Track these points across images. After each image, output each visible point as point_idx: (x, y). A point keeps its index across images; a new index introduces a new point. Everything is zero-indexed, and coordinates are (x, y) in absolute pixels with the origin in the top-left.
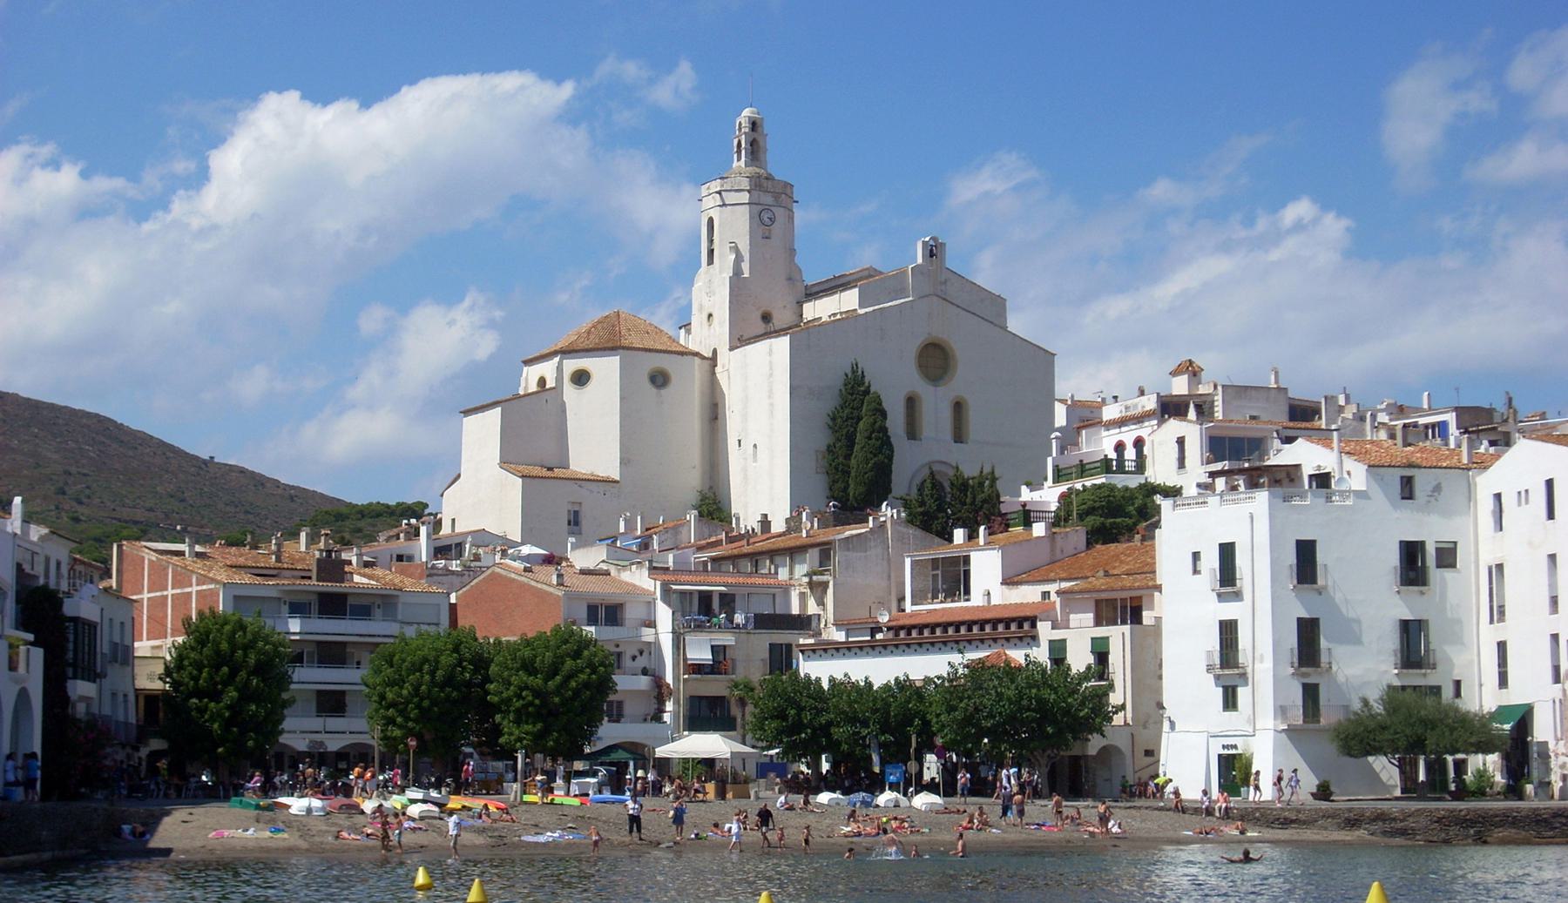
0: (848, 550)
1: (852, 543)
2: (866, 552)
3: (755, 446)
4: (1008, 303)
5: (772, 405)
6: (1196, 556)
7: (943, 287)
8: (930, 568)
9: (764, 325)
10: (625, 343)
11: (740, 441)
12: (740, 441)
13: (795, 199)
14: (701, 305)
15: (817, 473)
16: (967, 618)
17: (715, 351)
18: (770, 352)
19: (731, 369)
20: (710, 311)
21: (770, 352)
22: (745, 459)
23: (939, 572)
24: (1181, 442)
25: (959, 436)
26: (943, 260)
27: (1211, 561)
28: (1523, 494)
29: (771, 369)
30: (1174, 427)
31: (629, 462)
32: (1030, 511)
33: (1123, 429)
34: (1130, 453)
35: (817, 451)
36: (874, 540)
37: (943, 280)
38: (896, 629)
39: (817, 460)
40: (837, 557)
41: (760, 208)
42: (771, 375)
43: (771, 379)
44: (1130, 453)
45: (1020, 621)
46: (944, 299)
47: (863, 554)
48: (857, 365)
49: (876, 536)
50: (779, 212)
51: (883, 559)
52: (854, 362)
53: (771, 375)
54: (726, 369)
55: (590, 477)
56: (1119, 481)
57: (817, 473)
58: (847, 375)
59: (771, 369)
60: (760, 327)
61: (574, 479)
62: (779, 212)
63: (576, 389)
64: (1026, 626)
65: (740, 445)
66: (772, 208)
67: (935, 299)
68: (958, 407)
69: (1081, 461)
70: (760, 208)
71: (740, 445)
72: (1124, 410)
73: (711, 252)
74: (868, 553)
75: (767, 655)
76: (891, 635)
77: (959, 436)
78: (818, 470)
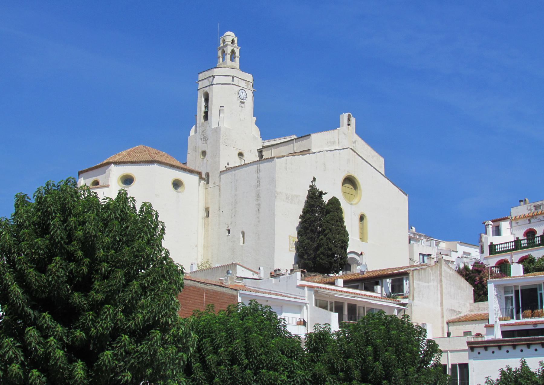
0: (420, 280)
3: (243, 233)
5: (259, 205)
7: (354, 145)
11: (229, 231)
12: (229, 231)
14: (196, 147)
15: (290, 251)
17: (208, 175)
18: (258, 171)
19: (221, 185)
20: (204, 149)
21: (258, 171)
29: (259, 181)
33: (532, 220)
35: (290, 236)
37: (354, 141)
39: (290, 242)
42: (259, 186)
43: (258, 188)
47: (427, 284)
49: (433, 272)
51: (437, 290)
59: (259, 181)
65: (229, 233)
68: (362, 218)
71: (229, 233)
72: (533, 209)
73: (206, 113)
74: (430, 284)
77: (363, 237)
78: (291, 250)
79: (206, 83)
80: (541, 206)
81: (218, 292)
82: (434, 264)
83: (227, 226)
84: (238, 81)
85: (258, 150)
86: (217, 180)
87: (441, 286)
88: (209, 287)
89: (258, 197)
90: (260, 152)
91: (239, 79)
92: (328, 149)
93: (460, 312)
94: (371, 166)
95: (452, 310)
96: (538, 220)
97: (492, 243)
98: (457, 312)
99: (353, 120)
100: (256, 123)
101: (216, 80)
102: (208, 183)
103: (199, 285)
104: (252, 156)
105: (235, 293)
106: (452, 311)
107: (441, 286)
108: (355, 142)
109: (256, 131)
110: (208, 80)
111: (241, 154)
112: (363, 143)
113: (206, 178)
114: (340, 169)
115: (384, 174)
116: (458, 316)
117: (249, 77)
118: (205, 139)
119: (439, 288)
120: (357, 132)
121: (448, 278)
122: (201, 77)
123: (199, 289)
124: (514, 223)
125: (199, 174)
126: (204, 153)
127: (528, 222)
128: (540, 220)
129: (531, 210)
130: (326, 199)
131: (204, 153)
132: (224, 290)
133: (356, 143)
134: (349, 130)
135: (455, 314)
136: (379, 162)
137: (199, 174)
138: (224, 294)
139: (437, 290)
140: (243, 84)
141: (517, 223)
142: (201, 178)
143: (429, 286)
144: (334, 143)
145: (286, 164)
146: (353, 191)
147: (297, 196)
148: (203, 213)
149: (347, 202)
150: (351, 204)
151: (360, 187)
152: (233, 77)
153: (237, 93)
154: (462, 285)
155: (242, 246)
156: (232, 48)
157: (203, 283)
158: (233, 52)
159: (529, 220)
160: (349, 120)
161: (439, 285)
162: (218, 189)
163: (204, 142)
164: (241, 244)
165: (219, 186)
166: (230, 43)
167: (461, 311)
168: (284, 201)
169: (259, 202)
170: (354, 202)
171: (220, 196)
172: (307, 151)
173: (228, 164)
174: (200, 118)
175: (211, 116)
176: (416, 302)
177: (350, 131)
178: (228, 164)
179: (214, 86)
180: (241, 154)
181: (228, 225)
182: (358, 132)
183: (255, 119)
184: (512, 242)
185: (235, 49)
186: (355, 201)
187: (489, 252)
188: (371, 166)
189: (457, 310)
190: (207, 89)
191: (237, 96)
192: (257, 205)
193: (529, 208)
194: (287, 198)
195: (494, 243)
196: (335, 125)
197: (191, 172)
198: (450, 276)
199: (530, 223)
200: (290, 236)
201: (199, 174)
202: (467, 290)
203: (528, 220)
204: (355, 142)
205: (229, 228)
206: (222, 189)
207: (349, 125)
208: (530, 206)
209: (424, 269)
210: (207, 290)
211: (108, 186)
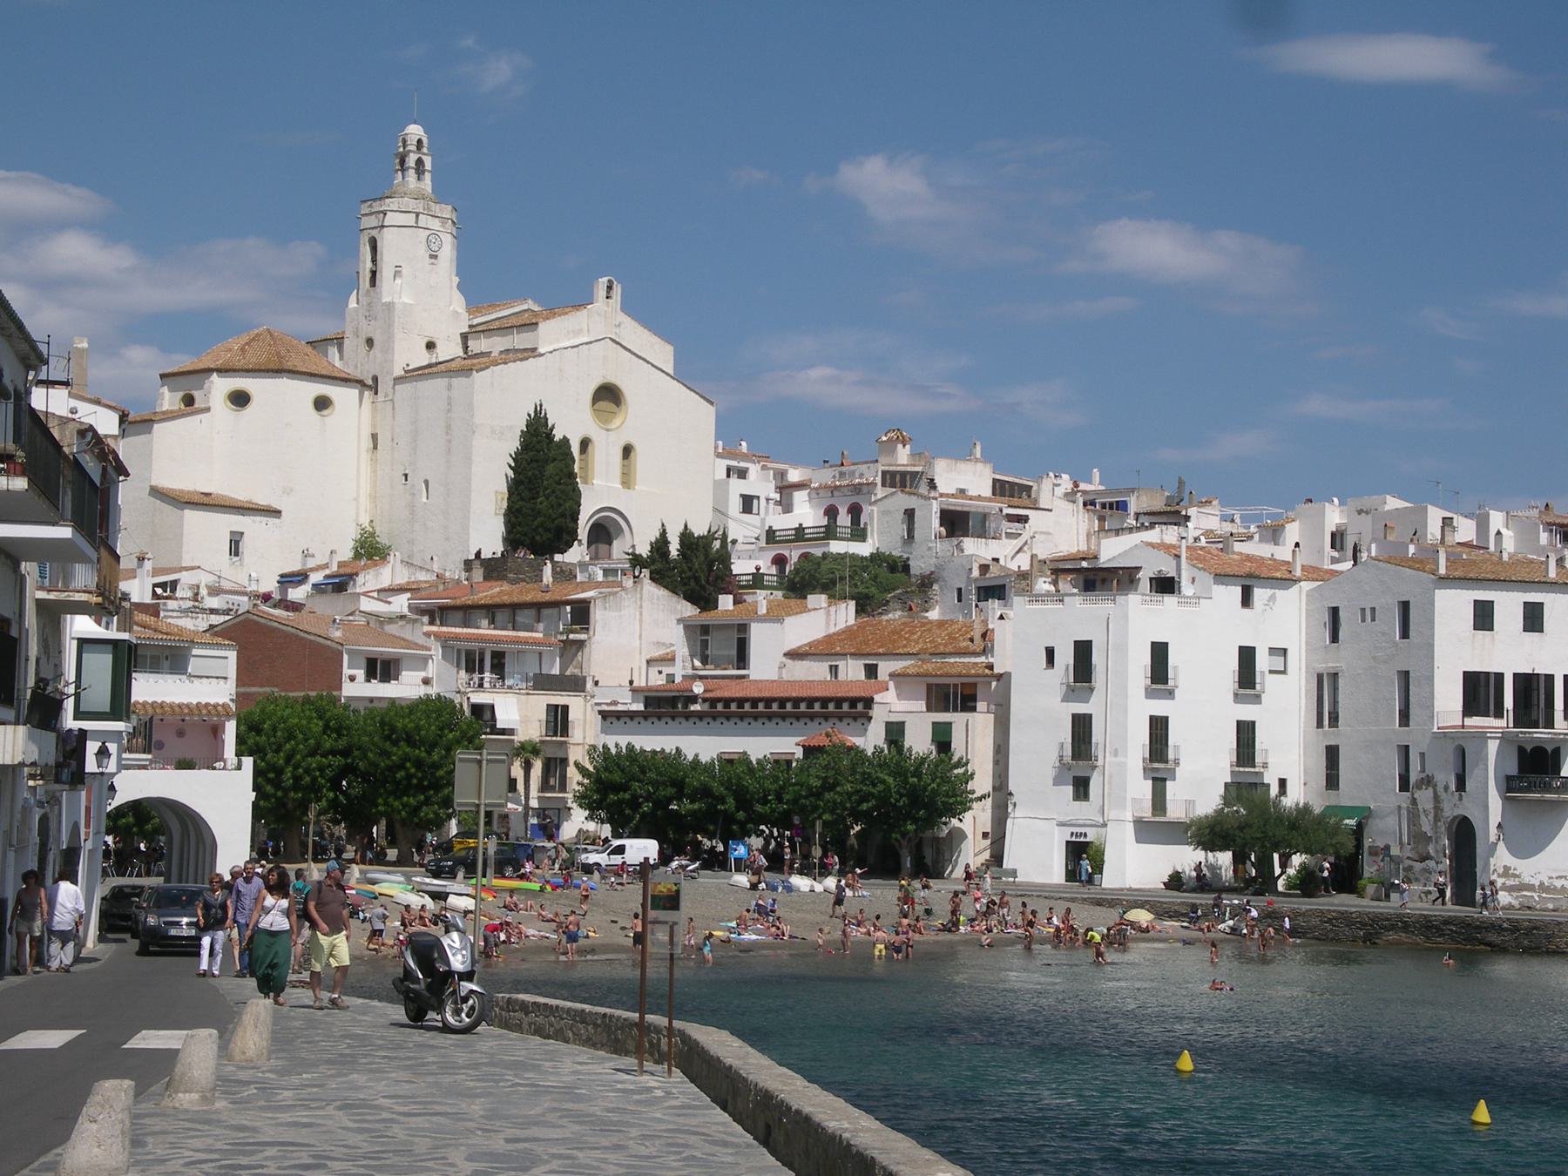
0: (605, 609)
3: (426, 482)
6: (1050, 653)
8: (699, 633)
9: (428, 356)
10: (289, 365)
11: (406, 475)
12: (406, 475)
15: (496, 514)
16: (766, 694)
17: (375, 379)
18: (449, 388)
19: (395, 400)
21: (449, 388)
24: (910, 514)
25: (627, 480)
27: (1065, 657)
28: (1368, 613)
29: (449, 404)
30: (902, 501)
31: (291, 490)
32: (763, 574)
33: (836, 493)
34: (844, 519)
35: (496, 492)
38: (713, 702)
40: (598, 614)
42: (449, 411)
44: (844, 519)
45: (853, 702)
46: (618, 343)
47: (617, 614)
48: (541, 406)
52: (538, 404)
53: (449, 411)
54: (390, 398)
55: (248, 505)
56: (836, 547)
57: (496, 514)
58: (529, 415)
59: (449, 404)
61: (238, 508)
63: (233, 410)
64: (860, 706)
68: (627, 451)
69: (801, 525)
72: (837, 475)
73: (374, 273)
74: (623, 612)
75: (544, 717)
76: (706, 707)
77: (627, 480)
79: (372, 221)
83: (402, 468)
86: (390, 391)
87: (641, 614)
88: (312, 638)
89: (448, 427)
92: (568, 344)
94: (648, 362)
97: (770, 527)
99: (617, 290)
100: (459, 287)
101: (391, 219)
102: (376, 393)
103: (302, 634)
104: (449, 349)
105: (340, 648)
106: (659, 644)
107: (641, 614)
109: (458, 303)
111: (430, 346)
112: (635, 324)
115: (671, 372)
117: (446, 211)
119: (638, 617)
120: (623, 309)
121: (655, 601)
122: (365, 209)
123: (302, 639)
125: (360, 383)
126: (370, 342)
131: (370, 342)
132: (329, 643)
133: (622, 326)
134: (608, 306)
136: (662, 353)
137: (360, 383)
139: (635, 619)
140: (435, 224)
143: (620, 617)
144: (579, 332)
146: (611, 406)
148: (367, 443)
149: (601, 428)
150: (608, 430)
152: (417, 215)
157: (306, 632)
158: (420, 162)
160: (610, 288)
161: (638, 613)
164: (424, 500)
165: (392, 400)
171: (394, 417)
172: (532, 352)
173: (408, 365)
174: (364, 281)
175: (381, 281)
178: (408, 365)
179: (385, 229)
180: (430, 346)
182: (626, 308)
183: (456, 280)
185: (424, 157)
186: (617, 422)
188: (648, 362)
190: (374, 233)
195: (774, 528)
196: (581, 301)
197: (345, 381)
198: (658, 599)
199: (833, 496)
200: (496, 492)
204: (619, 325)
209: (617, 592)
210: (311, 641)
211: (208, 410)
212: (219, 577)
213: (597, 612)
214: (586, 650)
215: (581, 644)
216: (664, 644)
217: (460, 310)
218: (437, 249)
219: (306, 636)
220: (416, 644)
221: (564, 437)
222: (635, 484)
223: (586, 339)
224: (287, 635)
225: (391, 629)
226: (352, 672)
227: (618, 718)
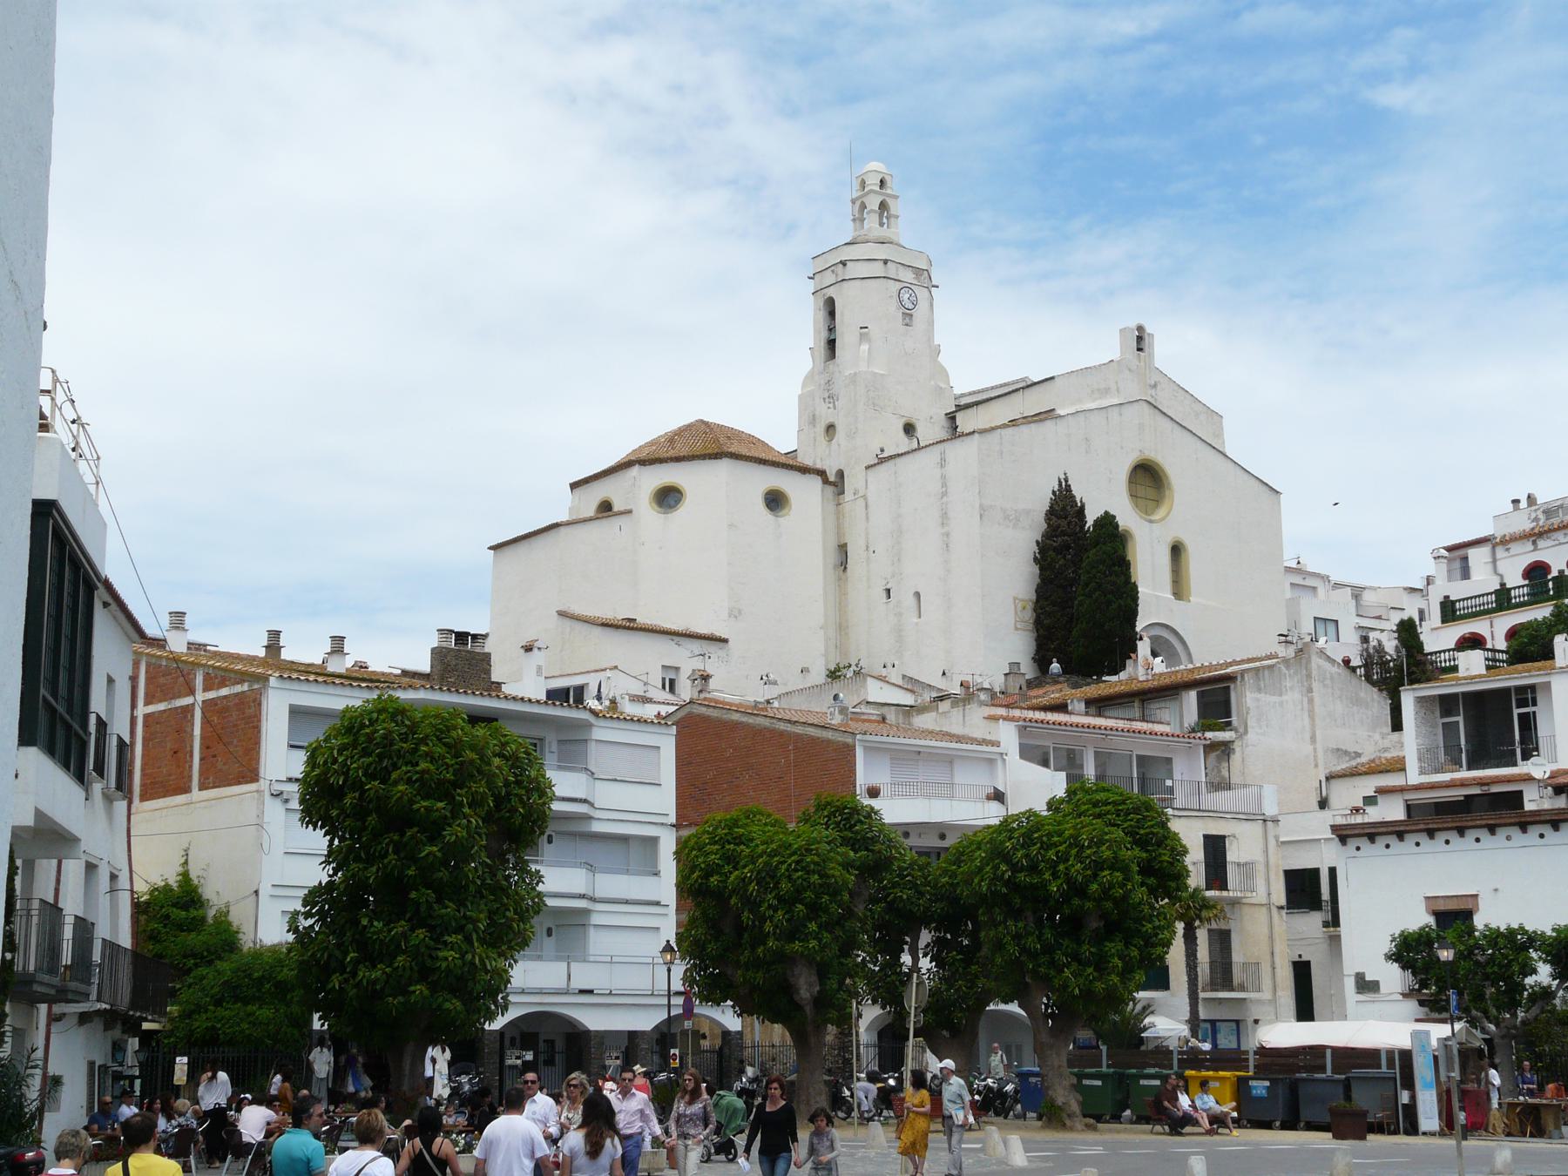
0: (1259, 690)
1: (1264, 680)
2: (1281, 695)
3: (917, 595)
4: (1225, 422)
5: (947, 535)
8: (1438, 713)
11: (888, 591)
12: (888, 591)
13: (934, 283)
14: (814, 416)
15: (1016, 629)
17: (841, 474)
18: (943, 463)
21: (943, 463)
22: (900, 615)
23: (1460, 719)
25: (1179, 589)
26: (1151, 356)
29: (944, 485)
31: (740, 612)
33: (1541, 543)
35: (1015, 599)
36: (1290, 675)
39: (1016, 613)
41: (900, 285)
42: (944, 494)
43: (945, 499)
47: (1275, 699)
48: (1066, 481)
50: (922, 294)
51: (1302, 709)
52: (1062, 477)
53: (944, 494)
57: (1016, 629)
59: (944, 485)
60: (903, 443)
62: (922, 294)
66: (912, 287)
67: (1145, 405)
68: (1177, 550)
70: (900, 285)
72: (1542, 517)
74: (1285, 698)
77: (1179, 589)
80: (1560, 511)
81: (818, 738)
82: (1293, 655)
83: (884, 582)
84: (897, 268)
85: (946, 414)
88: (799, 730)
89: (945, 518)
90: (951, 418)
91: (901, 267)
93: (1358, 755)
95: (1338, 750)
96: (1554, 543)
98: (1350, 753)
103: (782, 726)
105: (849, 740)
106: (1341, 752)
107: (1311, 701)
108: (1155, 386)
110: (833, 271)
111: (909, 429)
113: (835, 483)
114: (1122, 448)
116: (1354, 763)
118: (831, 398)
121: (1328, 682)
123: (782, 734)
124: (1500, 552)
125: (821, 473)
126: (830, 428)
127: (1532, 548)
128: (1557, 542)
129: (1536, 519)
130: (1091, 517)
132: (829, 735)
133: (1159, 387)
135: (1347, 758)
138: (829, 741)
140: (908, 276)
141: (1508, 550)
142: (826, 481)
143: (1281, 704)
145: (1001, 444)
146: (1151, 493)
147: (1028, 512)
149: (1141, 517)
150: (1151, 522)
151: (1169, 484)
153: (896, 294)
154: (1362, 695)
155: (917, 624)
156: (880, 199)
157: (789, 721)
159: (1534, 543)
161: (1306, 700)
162: (864, 504)
163: (831, 405)
164: (915, 620)
165: (864, 497)
166: (877, 188)
167: (1360, 751)
168: (999, 524)
169: (946, 529)
170: (1155, 517)
171: (867, 518)
173: (882, 450)
176: (1251, 736)
177: (1142, 364)
178: (882, 450)
180: (909, 429)
181: (885, 579)
184: (1491, 594)
185: (888, 200)
187: (1442, 617)
189: (1352, 750)
190: (831, 292)
191: (894, 302)
192: (943, 534)
193: (1533, 515)
194: (1007, 517)
199: (1536, 549)
201: (821, 476)
202: (1376, 704)
203: (1530, 543)
204: (1155, 386)
205: (888, 587)
206: (870, 503)
207: (1139, 349)
208: (1536, 510)
209: (1271, 667)
212: (645, 684)
213: (1248, 694)
214: (1236, 758)
215: (1224, 749)
216: (1346, 753)
217: (943, 386)
218: (911, 306)
219: (789, 728)
220: (976, 740)
221: (1106, 513)
222: (1189, 595)
223: (1116, 401)
224: (758, 732)
225: (924, 721)
226: (874, 781)
227: (1372, 838)
